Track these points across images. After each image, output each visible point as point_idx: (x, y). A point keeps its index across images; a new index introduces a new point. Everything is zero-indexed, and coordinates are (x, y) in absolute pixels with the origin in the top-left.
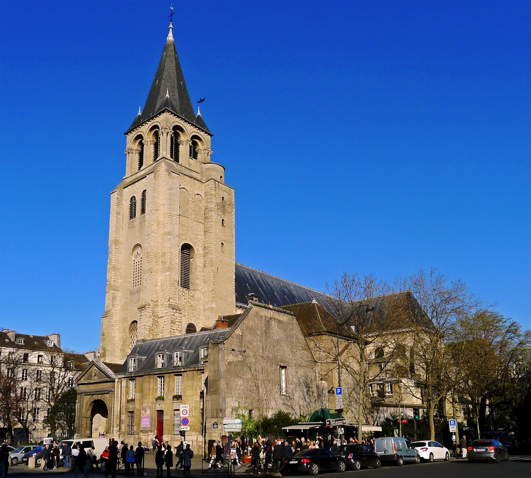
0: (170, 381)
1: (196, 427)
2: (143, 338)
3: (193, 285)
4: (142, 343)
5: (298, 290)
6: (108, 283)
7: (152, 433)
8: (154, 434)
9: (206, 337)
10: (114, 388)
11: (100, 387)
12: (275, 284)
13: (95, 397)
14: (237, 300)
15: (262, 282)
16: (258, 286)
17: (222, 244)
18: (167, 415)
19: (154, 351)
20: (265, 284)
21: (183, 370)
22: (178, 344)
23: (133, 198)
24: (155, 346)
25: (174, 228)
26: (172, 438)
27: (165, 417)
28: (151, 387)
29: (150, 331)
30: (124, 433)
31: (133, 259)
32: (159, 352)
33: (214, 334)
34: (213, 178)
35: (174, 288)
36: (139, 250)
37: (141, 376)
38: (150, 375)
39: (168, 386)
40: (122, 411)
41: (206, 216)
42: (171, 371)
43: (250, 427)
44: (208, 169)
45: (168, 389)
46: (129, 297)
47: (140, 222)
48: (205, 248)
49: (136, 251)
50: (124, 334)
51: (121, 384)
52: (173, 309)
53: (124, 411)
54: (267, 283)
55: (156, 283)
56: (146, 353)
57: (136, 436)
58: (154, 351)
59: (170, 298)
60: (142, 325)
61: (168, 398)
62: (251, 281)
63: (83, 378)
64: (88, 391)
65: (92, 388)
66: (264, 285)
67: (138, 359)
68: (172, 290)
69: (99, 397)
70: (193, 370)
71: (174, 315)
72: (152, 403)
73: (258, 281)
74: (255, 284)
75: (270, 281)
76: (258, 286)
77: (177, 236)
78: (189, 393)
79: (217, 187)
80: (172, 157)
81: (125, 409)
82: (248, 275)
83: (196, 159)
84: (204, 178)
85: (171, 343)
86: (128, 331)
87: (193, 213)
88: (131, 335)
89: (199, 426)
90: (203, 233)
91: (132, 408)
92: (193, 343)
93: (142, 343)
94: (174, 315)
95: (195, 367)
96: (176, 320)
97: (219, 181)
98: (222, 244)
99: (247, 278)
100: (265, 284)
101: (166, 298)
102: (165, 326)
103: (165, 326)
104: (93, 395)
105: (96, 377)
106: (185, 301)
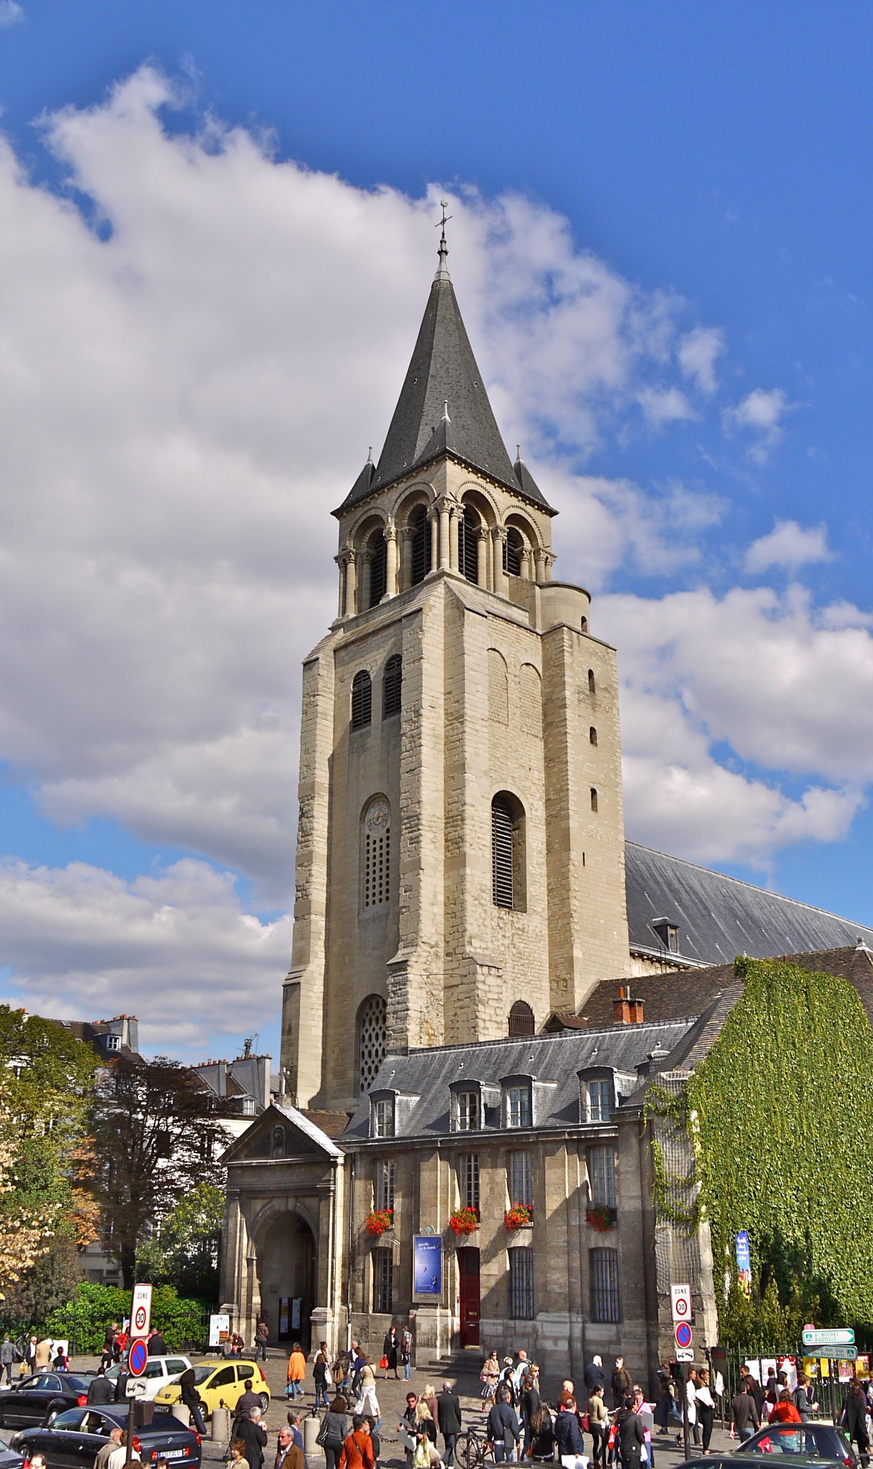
1: (578, 1300)
3: (523, 898)
5: (764, 903)
8: (453, 1314)
9: (588, 1046)
12: (708, 889)
14: (632, 939)
15: (677, 885)
16: (670, 896)
17: (594, 792)
19: (439, 1081)
20: (686, 891)
22: (508, 1065)
23: (362, 676)
24: (442, 1066)
25: (477, 754)
26: (506, 1327)
29: (422, 1024)
31: (367, 832)
33: (611, 1037)
34: (565, 622)
35: (480, 910)
41: (550, 719)
43: (714, 1297)
44: (549, 598)
45: (492, 1190)
46: (357, 930)
47: (382, 738)
48: (549, 803)
49: (372, 810)
52: (481, 965)
54: (691, 888)
55: (435, 896)
56: (418, 1083)
58: (439, 1081)
59: (471, 938)
61: (491, 1215)
62: (651, 883)
63: (245, 1152)
66: (684, 895)
67: (401, 1102)
68: (477, 915)
71: (484, 982)
73: (669, 884)
74: (662, 890)
75: (695, 883)
76: (670, 896)
77: (486, 773)
79: (575, 646)
80: (460, 571)
82: (643, 867)
83: (518, 573)
84: (539, 622)
85: (488, 1061)
86: (353, 1021)
87: (518, 712)
89: (582, 1296)
90: (541, 764)
92: (552, 1064)
93: (401, 1057)
94: (484, 982)
96: (490, 996)
97: (580, 629)
98: (594, 792)
99: (642, 877)
100: (686, 891)
102: (459, 1011)
106: (506, 942)
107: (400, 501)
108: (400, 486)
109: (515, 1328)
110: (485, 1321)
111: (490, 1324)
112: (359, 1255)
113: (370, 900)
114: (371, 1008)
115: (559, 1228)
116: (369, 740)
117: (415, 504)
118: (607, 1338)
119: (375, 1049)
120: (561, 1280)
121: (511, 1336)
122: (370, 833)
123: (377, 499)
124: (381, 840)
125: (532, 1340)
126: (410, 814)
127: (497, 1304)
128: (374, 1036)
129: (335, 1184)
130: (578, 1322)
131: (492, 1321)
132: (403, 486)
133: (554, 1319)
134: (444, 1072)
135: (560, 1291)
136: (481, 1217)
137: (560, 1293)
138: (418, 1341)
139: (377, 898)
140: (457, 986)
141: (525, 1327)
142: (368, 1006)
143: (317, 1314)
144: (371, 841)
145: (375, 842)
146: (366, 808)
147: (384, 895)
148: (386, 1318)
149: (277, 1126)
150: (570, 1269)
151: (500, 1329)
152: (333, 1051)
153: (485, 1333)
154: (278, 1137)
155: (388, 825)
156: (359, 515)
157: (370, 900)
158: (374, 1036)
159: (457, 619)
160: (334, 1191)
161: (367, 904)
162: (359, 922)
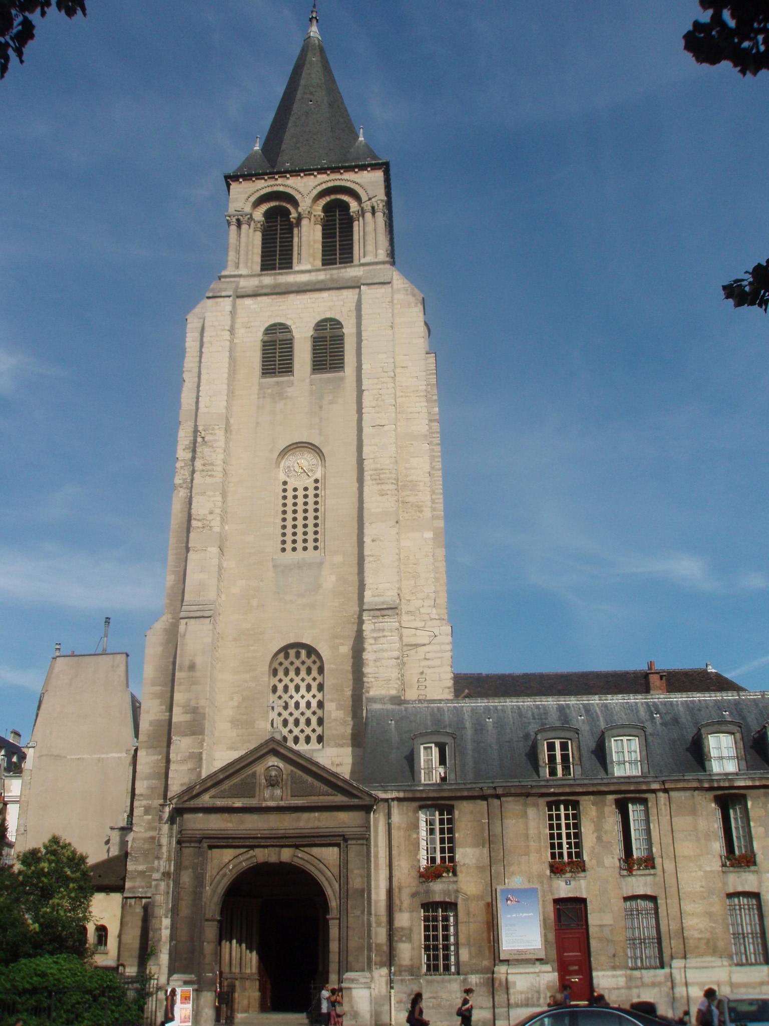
0: (601, 816)
1: (721, 944)
2: (393, 692)
4: (390, 707)
6: (200, 524)
7: (548, 968)
10: (368, 828)
11: (302, 824)
13: (262, 855)
18: (601, 911)
21: (655, 786)
26: (630, 978)
27: (593, 919)
28: (532, 832)
30: (413, 971)
31: (282, 477)
32: (553, 734)
36: (305, 460)
37: (484, 798)
38: (528, 795)
39: (598, 828)
40: (397, 901)
42: (612, 788)
45: (599, 838)
50: (247, 676)
51: (389, 816)
53: (404, 899)
57: (474, 979)
60: (386, 655)
61: (600, 863)
63: (212, 792)
64: (240, 833)
65: (253, 824)
69: (286, 855)
70: (695, 789)
72: (540, 876)
78: (685, 848)
81: (414, 895)
86: (266, 668)
88: (275, 681)
91: (447, 893)
95: (700, 781)
101: (428, 597)
103: (426, 670)
104: (252, 847)
105: (278, 792)
107: (319, 189)
108: (319, 176)
109: (641, 978)
110: (600, 973)
111: (608, 976)
112: (401, 910)
113: (289, 545)
114: (287, 656)
115: (694, 874)
116: (289, 389)
117: (333, 197)
118: (758, 980)
119: (294, 701)
120: (701, 926)
121: (637, 987)
122: (287, 479)
123: (288, 178)
124: (306, 489)
125: (666, 988)
126: (379, 466)
127: (614, 956)
128: (292, 687)
129: (370, 831)
130: (723, 966)
131: (610, 973)
132: (322, 177)
133: (698, 965)
134: (468, 725)
135: (700, 936)
136: (587, 865)
137: (700, 939)
138: (512, 1001)
139: (300, 545)
140: (424, 645)
141: (655, 976)
142: (282, 655)
143: (352, 980)
144: (289, 488)
145: (295, 490)
146: (284, 453)
147: (310, 544)
148: (450, 981)
149: (270, 764)
150: (710, 915)
151: (622, 981)
152: (232, 699)
153: (601, 986)
154: (276, 776)
155: (318, 475)
156: (262, 186)
157: (289, 545)
158: (292, 687)
159: (413, 305)
160: (368, 839)
161: (284, 550)
162: (275, 566)
